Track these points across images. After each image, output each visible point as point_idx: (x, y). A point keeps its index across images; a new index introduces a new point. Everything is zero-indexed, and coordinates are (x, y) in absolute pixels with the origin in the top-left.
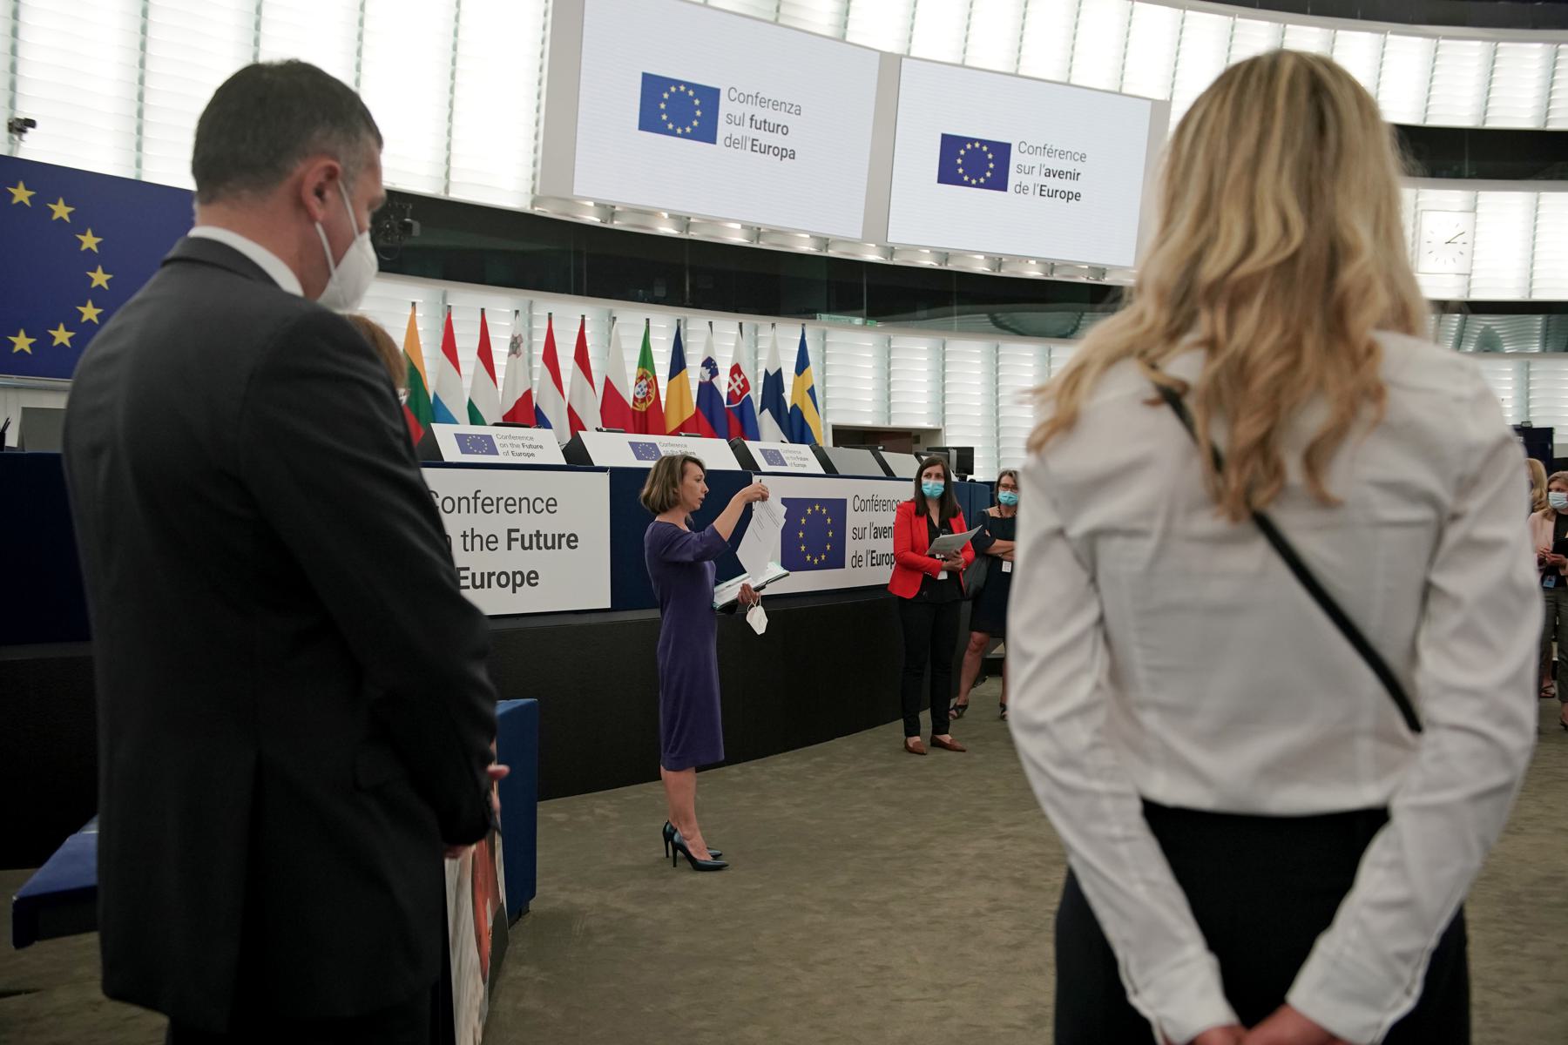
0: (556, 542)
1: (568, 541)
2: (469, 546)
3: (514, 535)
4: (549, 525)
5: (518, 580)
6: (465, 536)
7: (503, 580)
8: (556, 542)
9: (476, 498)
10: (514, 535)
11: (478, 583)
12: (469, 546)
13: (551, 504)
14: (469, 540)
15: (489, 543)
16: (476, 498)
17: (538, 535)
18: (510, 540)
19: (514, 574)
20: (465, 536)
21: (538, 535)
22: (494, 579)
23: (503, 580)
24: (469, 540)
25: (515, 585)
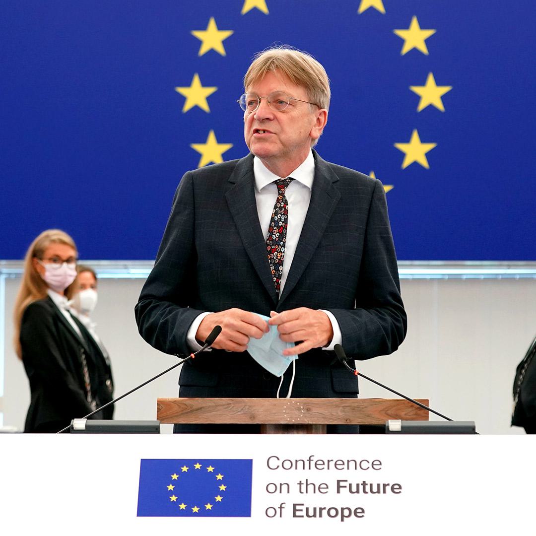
0: (381, 489)
1: (393, 489)
2: (304, 490)
3: (342, 484)
4: (373, 477)
5: (346, 513)
6: (300, 484)
7: (333, 512)
8: (381, 489)
9: (310, 460)
10: (342, 484)
11: (311, 513)
12: (304, 490)
13: (376, 465)
14: (304, 487)
15: (321, 488)
16: (310, 460)
17: (364, 484)
18: (339, 487)
19: (342, 509)
20: (300, 484)
21: (364, 484)
22: (325, 512)
23: (333, 512)
24: (304, 487)
25: (343, 516)
